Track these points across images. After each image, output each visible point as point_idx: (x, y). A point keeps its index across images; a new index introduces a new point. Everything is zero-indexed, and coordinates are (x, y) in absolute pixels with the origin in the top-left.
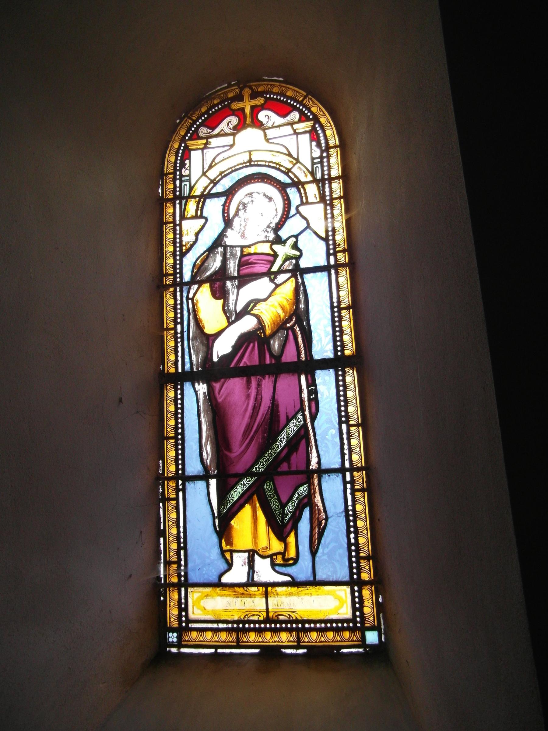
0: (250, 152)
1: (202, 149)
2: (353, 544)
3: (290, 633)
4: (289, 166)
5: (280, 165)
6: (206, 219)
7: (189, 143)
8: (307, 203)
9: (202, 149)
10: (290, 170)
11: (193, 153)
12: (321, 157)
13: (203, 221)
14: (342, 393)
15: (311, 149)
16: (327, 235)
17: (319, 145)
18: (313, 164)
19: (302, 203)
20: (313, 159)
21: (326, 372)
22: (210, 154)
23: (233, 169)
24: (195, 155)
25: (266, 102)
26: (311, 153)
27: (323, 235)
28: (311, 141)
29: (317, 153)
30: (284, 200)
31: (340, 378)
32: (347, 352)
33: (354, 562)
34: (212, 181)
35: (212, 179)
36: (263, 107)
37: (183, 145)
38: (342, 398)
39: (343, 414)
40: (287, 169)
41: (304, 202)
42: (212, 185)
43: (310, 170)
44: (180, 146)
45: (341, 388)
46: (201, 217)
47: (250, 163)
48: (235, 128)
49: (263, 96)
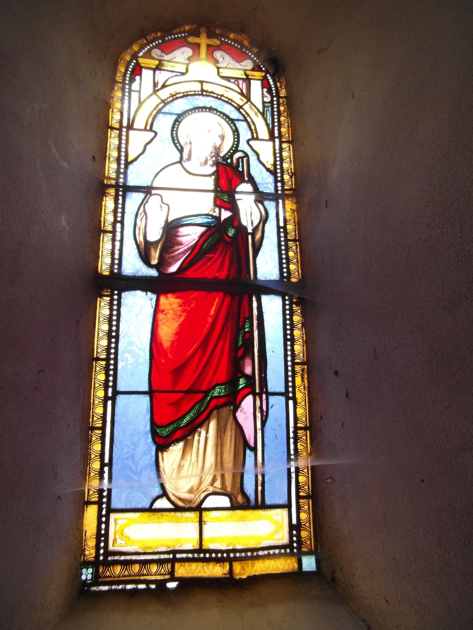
0: (202, 82)
1: (154, 70)
2: (282, 227)
3: (106, 349)
4: (241, 103)
5: (232, 101)
6: (156, 133)
7: (141, 61)
8: (257, 139)
9: (154, 70)
10: (241, 107)
11: (144, 71)
12: (272, 102)
13: (152, 134)
14: (288, 317)
15: (263, 94)
16: (276, 169)
17: (270, 92)
18: (264, 107)
19: (253, 139)
20: (264, 102)
21: (272, 297)
22: (161, 77)
23: (185, 94)
24: (147, 74)
25: (221, 44)
26: (263, 98)
27: (272, 168)
28: (263, 87)
29: (268, 99)
30: (234, 132)
31: (285, 266)
32: (294, 280)
33: (287, 310)
34: (163, 101)
35: (163, 98)
36: (218, 48)
37: (134, 61)
38: (288, 322)
39: (288, 322)
40: (238, 105)
41: (255, 137)
42: (162, 104)
43: (261, 111)
44: (131, 61)
45: (288, 327)
46: (151, 130)
47: (203, 93)
48: (189, 59)
49: (218, 38)
